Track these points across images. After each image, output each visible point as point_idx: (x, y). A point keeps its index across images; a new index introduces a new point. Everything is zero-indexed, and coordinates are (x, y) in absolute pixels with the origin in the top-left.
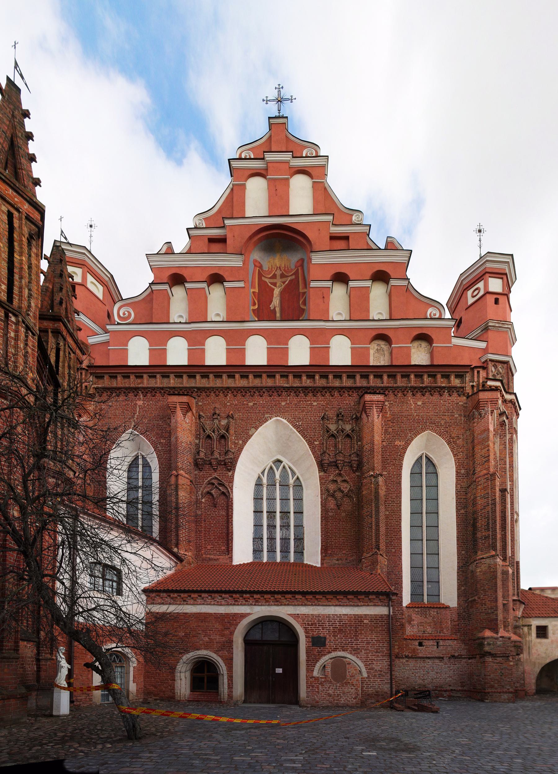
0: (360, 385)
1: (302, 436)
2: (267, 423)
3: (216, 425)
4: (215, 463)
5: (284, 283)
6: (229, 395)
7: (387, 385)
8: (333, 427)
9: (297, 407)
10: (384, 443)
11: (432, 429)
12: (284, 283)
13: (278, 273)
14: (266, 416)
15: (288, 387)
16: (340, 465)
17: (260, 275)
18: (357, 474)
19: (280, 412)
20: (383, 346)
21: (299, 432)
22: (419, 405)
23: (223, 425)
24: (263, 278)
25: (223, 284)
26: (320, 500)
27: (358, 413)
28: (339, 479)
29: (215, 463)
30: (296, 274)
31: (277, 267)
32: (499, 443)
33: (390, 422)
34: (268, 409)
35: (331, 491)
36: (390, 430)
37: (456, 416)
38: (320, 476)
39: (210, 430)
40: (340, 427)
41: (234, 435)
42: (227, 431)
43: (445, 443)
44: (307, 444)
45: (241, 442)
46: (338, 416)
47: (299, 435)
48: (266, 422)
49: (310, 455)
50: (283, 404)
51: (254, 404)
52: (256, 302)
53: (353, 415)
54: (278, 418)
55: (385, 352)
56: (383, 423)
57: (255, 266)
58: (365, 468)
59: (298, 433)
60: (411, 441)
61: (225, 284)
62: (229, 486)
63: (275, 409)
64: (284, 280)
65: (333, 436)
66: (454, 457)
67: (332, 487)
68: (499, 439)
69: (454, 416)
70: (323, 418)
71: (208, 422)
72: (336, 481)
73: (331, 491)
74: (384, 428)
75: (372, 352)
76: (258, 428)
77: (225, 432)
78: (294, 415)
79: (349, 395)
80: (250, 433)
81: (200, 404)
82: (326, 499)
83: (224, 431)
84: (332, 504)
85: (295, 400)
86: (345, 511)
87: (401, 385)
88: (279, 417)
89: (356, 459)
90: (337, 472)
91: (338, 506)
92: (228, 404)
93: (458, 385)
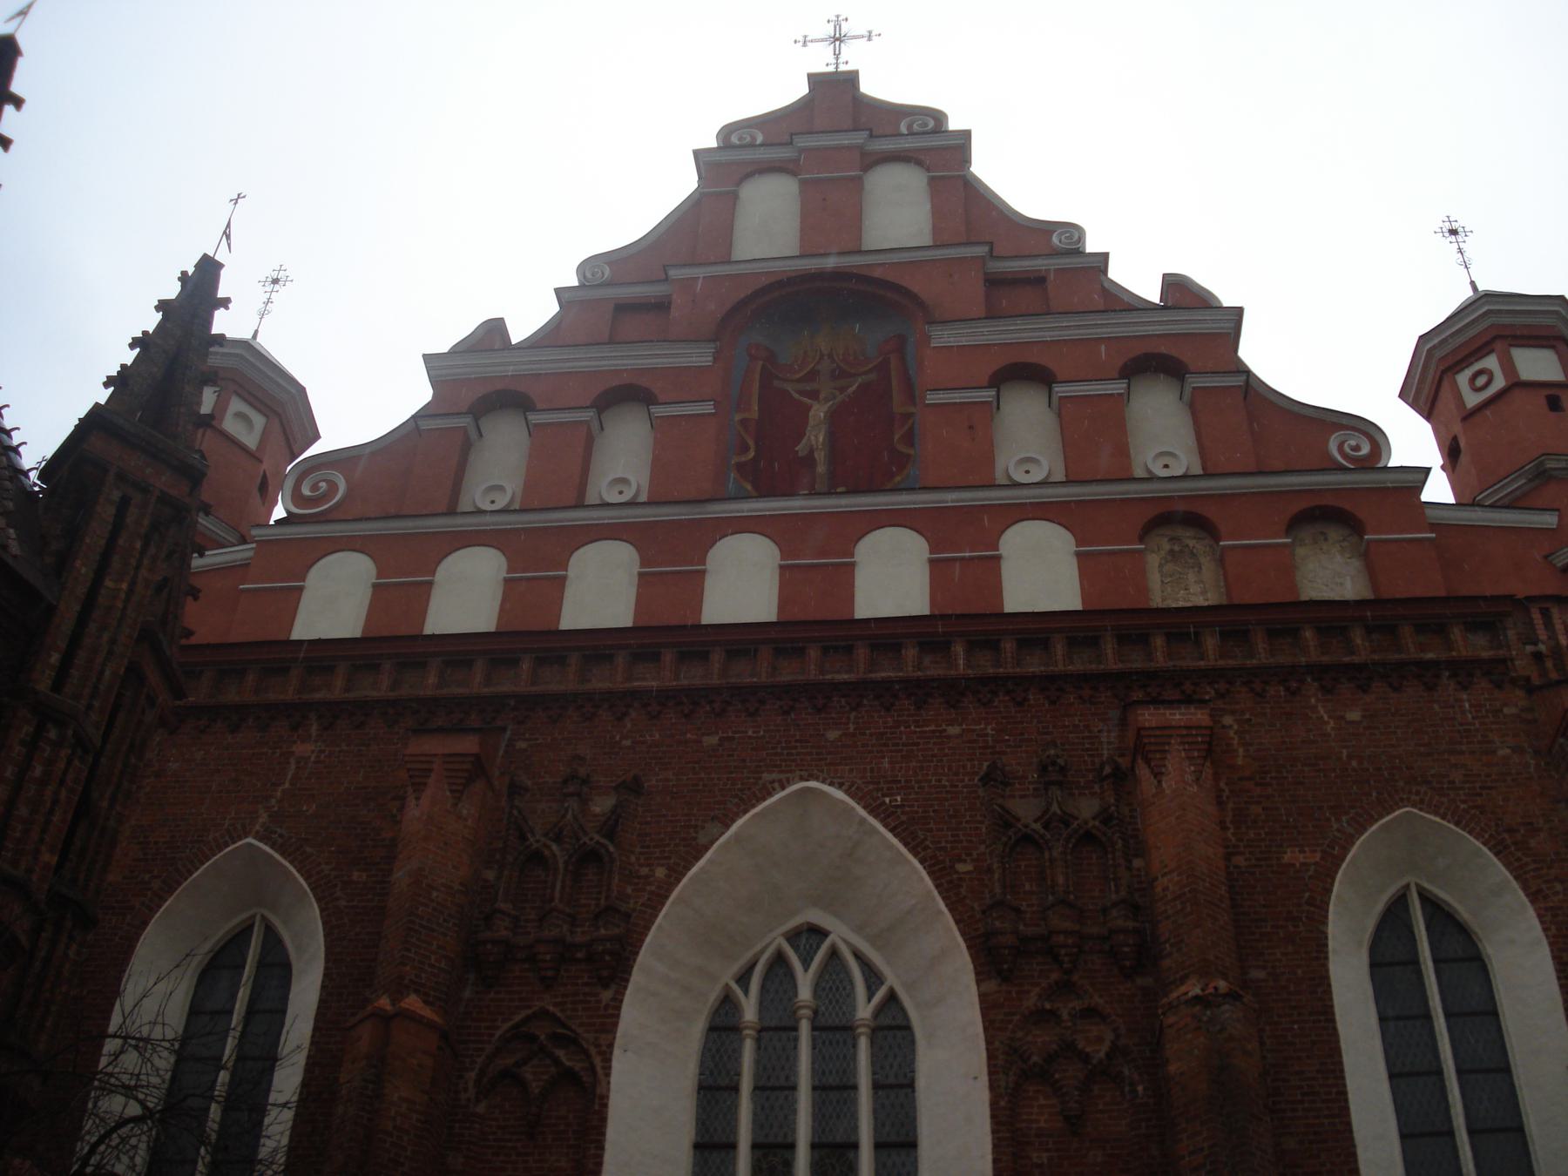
0: (1121, 666)
1: (906, 845)
3: (569, 816)
4: (548, 957)
5: (842, 390)
6: (633, 714)
7: (1221, 663)
8: (1026, 810)
9: (886, 745)
11: (1422, 801)
12: (842, 390)
14: (766, 777)
15: (851, 683)
16: (1063, 951)
18: (1140, 981)
20: (1191, 543)
21: (891, 830)
22: (1352, 722)
23: (595, 816)
24: (776, 383)
25: (649, 410)
27: (1122, 755)
29: (548, 957)
31: (822, 356)
34: (776, 754)
35: (1035, 1058)
38: (983, 997)
39: (546, 835)
40: (1055, 808)
41: (638, 850)
42: (611, 835)
43: (1485, 849)
44: (924, 873)
45: (660, 872)
46: (1043, 769)
47: (895, 841)
48: (764, 799)
49: (940, 912)
50: (832, 735)
51: (720, 740)
53: (1102, 765)
54: (813, 784)
55: (1203, 560)
56: (1222, 785)
58: (1167, 963)
59: (889, 836)
60: (1345, 850)
61: (653, 409)
62: (598, 1046)
63: (798, 754)
65: (1027, 839)
66: (1532, 902)
70: (987, 779)
72: (1053, 1013)
73: (1035, 1058)
74: (1230, 805)
75: (1153, 560)
76: (733, 821)
77: (603, 841)
78: (872, 770)
79: (1080, 697)
80: (702, 840)
83: (597, 837)
87: (1272, 660)
88: (817, 779)
89: (1131, 924)
90: (1054, 976)
92: (627, 743)
93: (1485, 654)
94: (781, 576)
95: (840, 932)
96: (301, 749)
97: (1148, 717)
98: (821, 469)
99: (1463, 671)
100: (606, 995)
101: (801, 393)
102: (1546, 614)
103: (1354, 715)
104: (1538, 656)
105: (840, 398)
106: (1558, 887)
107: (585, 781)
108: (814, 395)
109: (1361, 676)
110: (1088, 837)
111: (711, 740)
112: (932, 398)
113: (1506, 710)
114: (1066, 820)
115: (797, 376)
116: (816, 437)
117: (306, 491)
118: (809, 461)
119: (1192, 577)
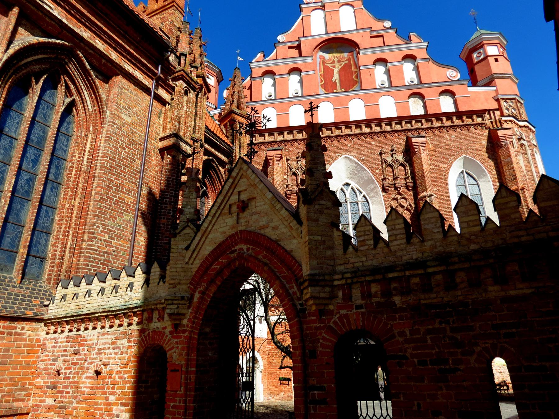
2: (338, 159)
8: (389, 159)
10: (431, 167)
12: (340, 65)
14: (337, 155)
17: (324, 63)
24: (326, 64)
28: (399, 197)
32: (522, 160)
33: (433, 152)
36: (434, 157)
50: (349, 145)
52: (323, 79)
54: (346, 156)
57: (320, 59)
65: (390, 165)
68: (522, 157)
69: (481, 143)
70: (381, 154)
71: (293, 163)
81: (287, 151)
85: (358, 142)
94: (335, 113)
98: (338, 84)
102: (494, 113)
103: (453, 136)
105: (340, 67)
108: (334, 67)
113: (484, 134)
114: (397, 161)
115: (330, 62)
118: (335, 82)
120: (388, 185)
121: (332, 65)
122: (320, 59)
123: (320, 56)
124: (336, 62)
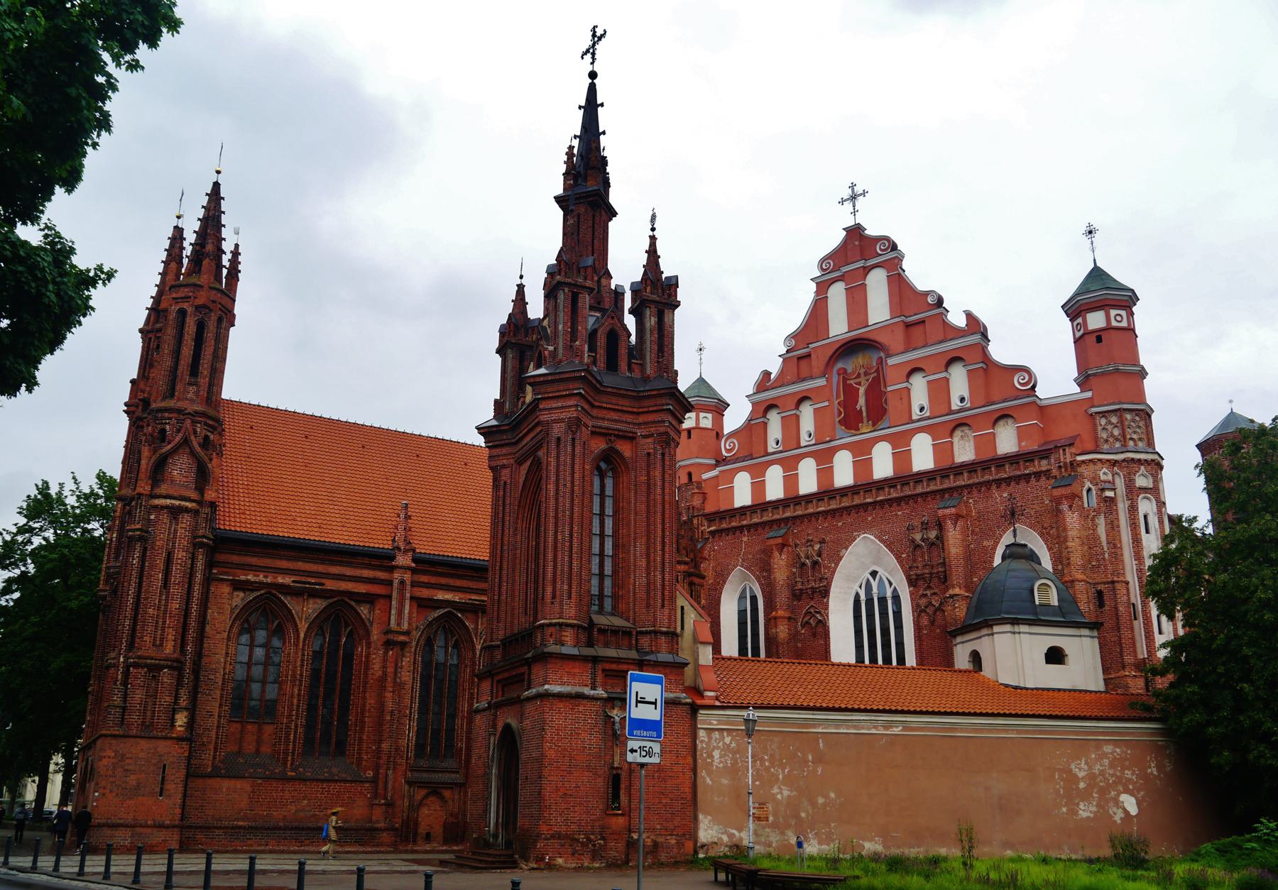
5: (868, 380)
8: (918, 537)
12: (868, 380)
13: (862, 371)
17: (845, 380)
19: (867, 528)
24: (848, 382)
26: (912, 618)
28: (928, 592)
30: (877, 371)
33: (976, 521)
36: (977, 530)
37: (1047, 502)
45: (833, 565)
46: (922, 523)
50: (869, 519)
52: (842, 410)
64: (867, 377)
67: (923, 602)
82: (919, 615)
84: (925, 621)
86: (939, 627)
91: (932, 622)
95: (881, 572)
96: (745, 539)
97: (940, 512)
98: (864, 414)
99: (1038, 475)
100: (825, 600)
101: (856, 383)
102: (1064, 450)
104: (1060, 467)
106: (1057, 546)
107: (812, 541)
108: (859, 384)
109: (1008, 481)
110: (933, 544)
111: (840, 524)
112: (889, 389)
116: (862, 401)
117: (728, 447)
119: (967, 444)
120: (914, 577)
121: (857, 381)
122: (839, 375)
123: (840, 369)
124: (862, 375)
